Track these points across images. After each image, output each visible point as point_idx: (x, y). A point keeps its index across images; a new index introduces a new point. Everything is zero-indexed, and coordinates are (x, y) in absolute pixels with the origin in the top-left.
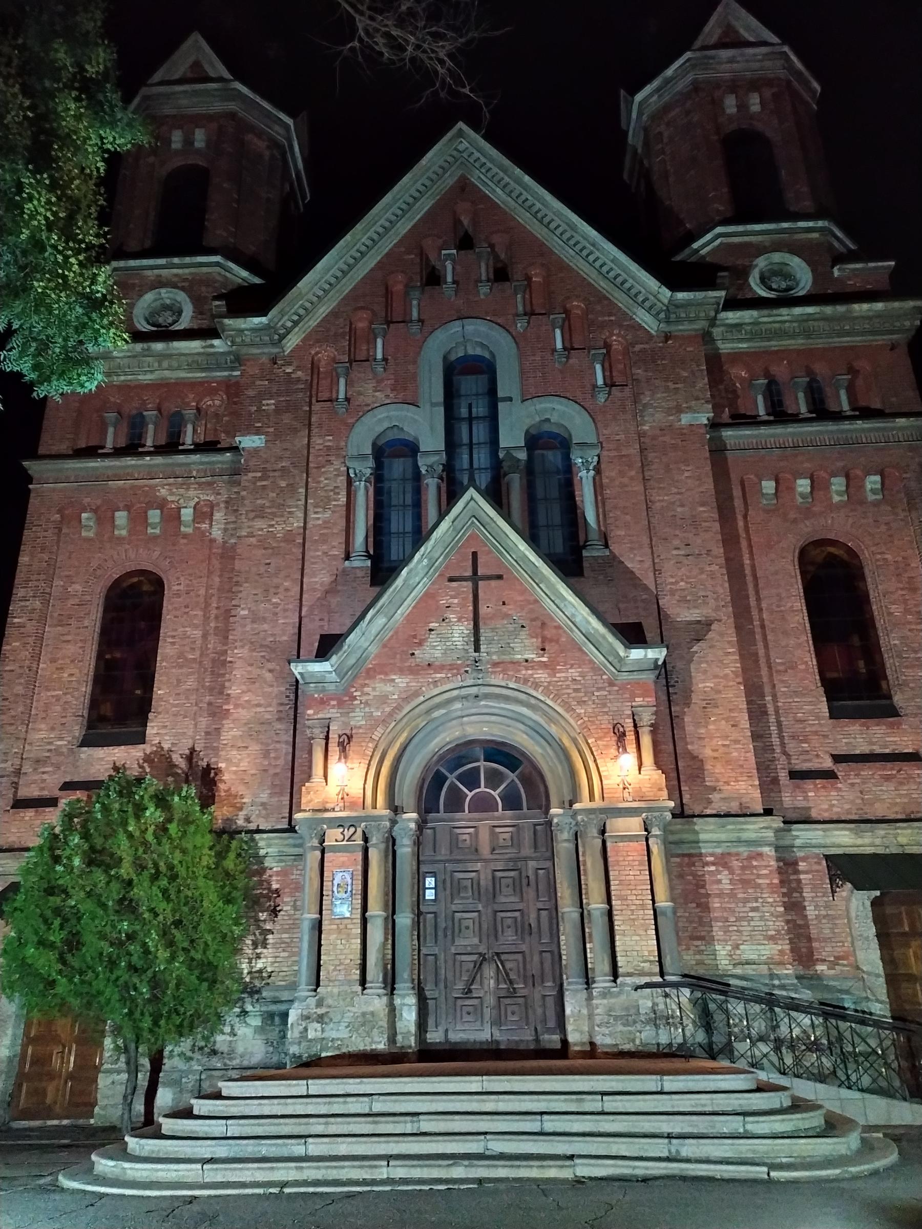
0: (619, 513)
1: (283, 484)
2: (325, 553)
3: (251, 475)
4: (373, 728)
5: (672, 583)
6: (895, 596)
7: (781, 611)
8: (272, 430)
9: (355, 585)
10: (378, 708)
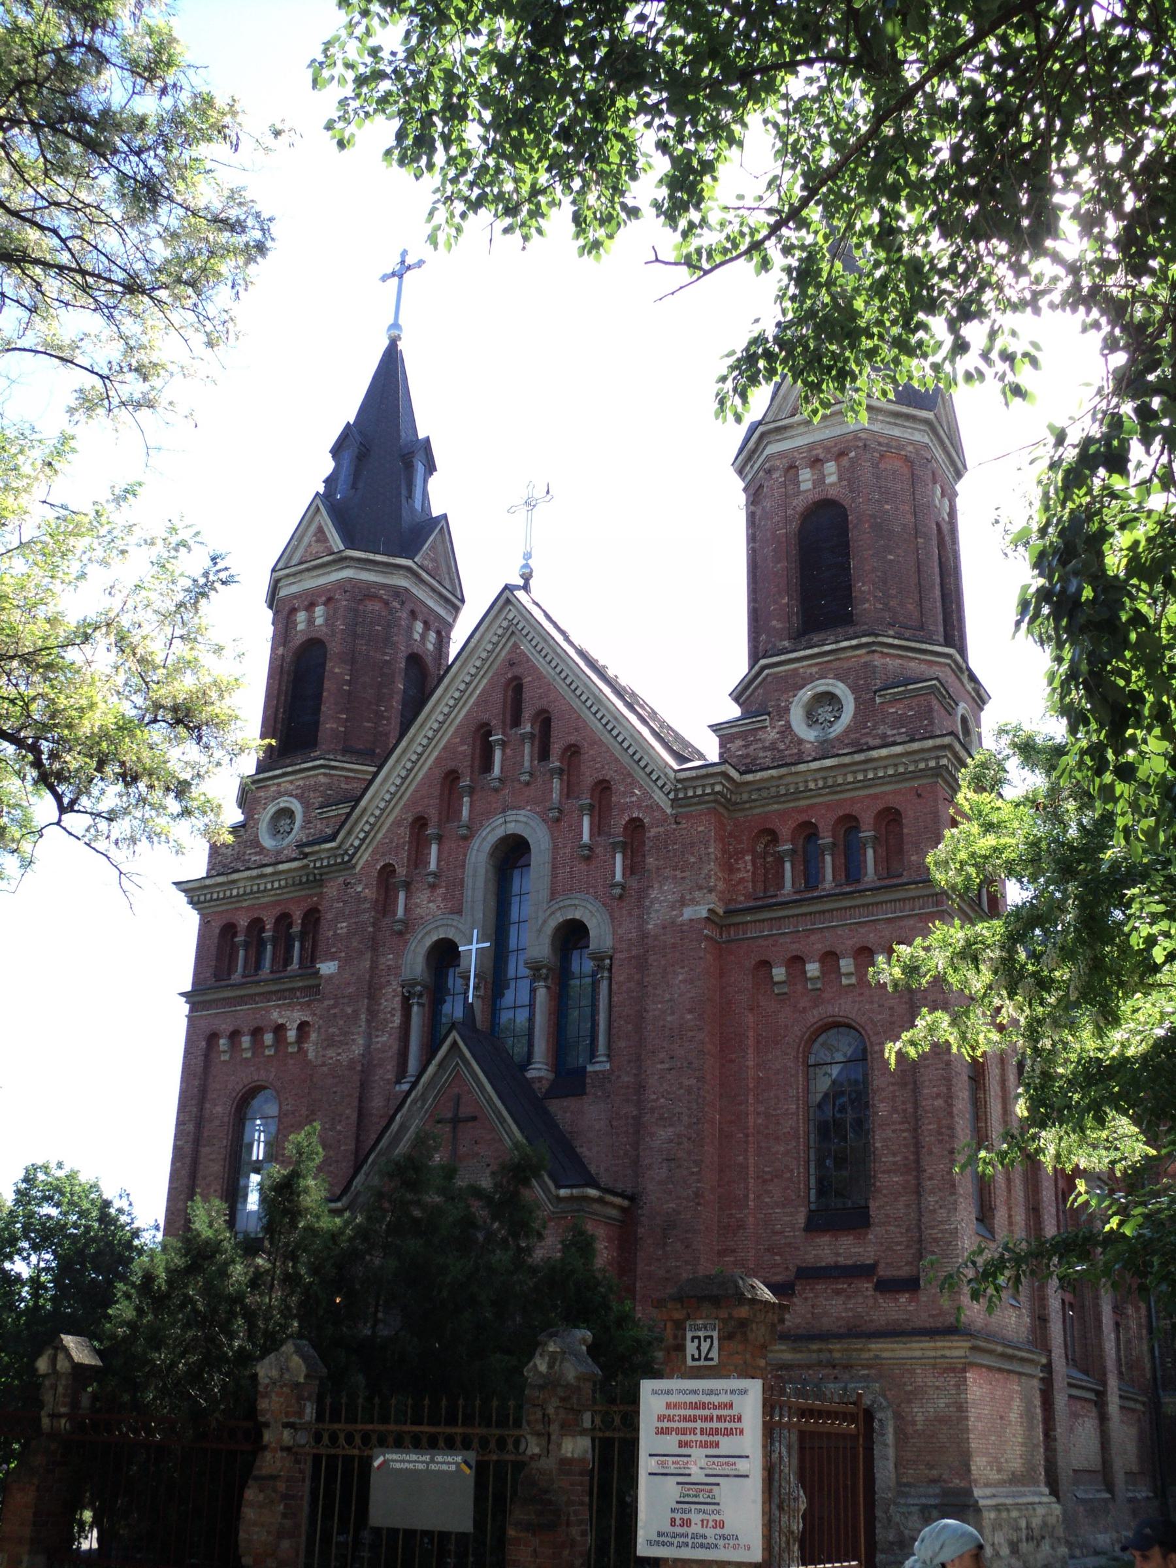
3: (327, 1003)
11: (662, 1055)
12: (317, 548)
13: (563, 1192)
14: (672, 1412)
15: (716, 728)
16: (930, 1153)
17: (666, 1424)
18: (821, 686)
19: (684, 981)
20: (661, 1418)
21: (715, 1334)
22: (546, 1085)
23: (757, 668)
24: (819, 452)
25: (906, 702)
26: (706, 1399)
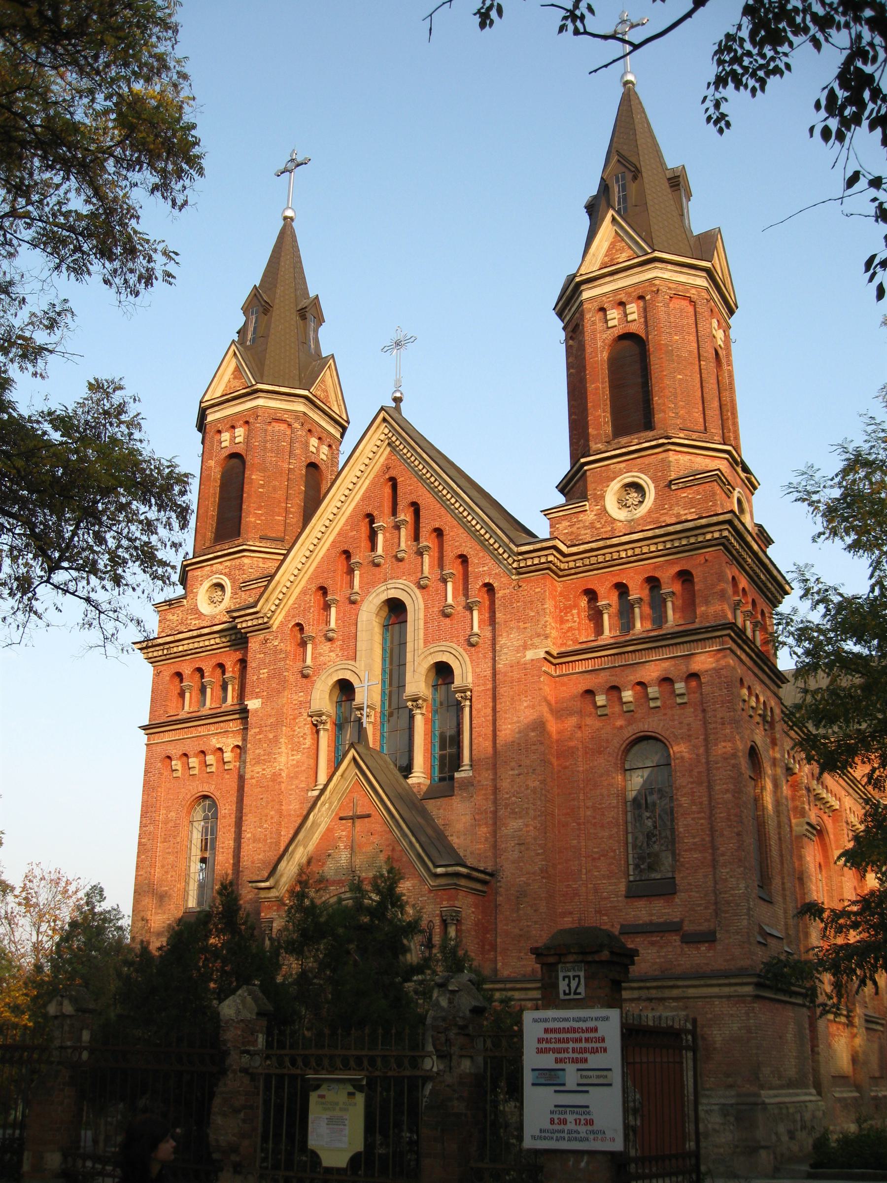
2: (297, 787)
5: (506, 799)
8: (265, 693)
11: (513, 764)
12: (237, 384)
13: (440, 870)
14: (549, 1036)
15: (546, 512)
17: (544, 1045)
18: (628, 478)
20: (540, 1041)
21: (582, 974)
22: (424, 788)
23: (578, 465)
24: (623, 297)
25: (695, 488)
26: (576, 1025)
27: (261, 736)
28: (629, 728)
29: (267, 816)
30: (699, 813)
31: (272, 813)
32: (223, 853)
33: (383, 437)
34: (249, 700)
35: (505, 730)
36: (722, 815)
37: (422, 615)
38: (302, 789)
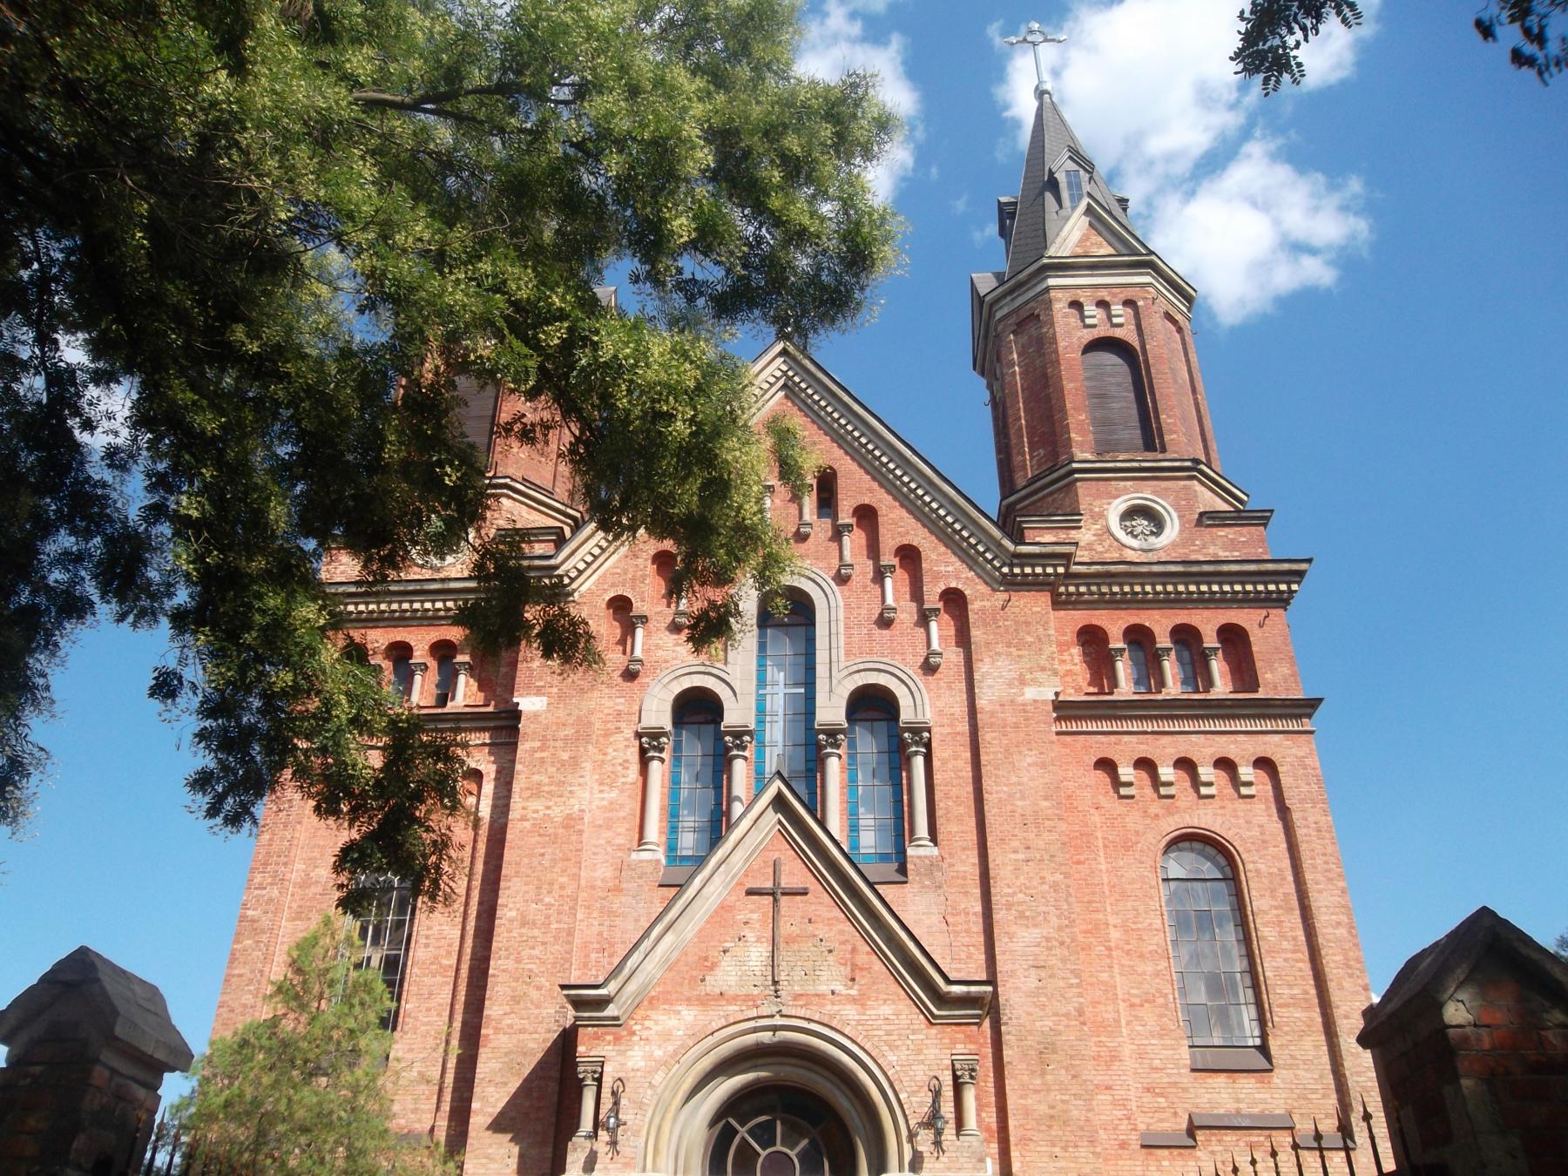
0: (950, 803)
1: (565, 756)
4: (652, 1072)
5: (1008, 895)
6: (1267, 918)
7: (1138, 929)
8: (555, 690)
9: (641, 882)
10: (659, 1046)
11: (1015, 844)
16: (1341, 988)
19: (1035, 764)
27: (543, 755)
28: (1170, 819)
29: (551, 884)
30: (1294, 952)
31: (563, 880)
32: (427, 946)
33: (778, 374)
34: (521, 696)
35: (997, 792)
36: (1337, 958)
37: (841, 616)
38: (619, 848)
